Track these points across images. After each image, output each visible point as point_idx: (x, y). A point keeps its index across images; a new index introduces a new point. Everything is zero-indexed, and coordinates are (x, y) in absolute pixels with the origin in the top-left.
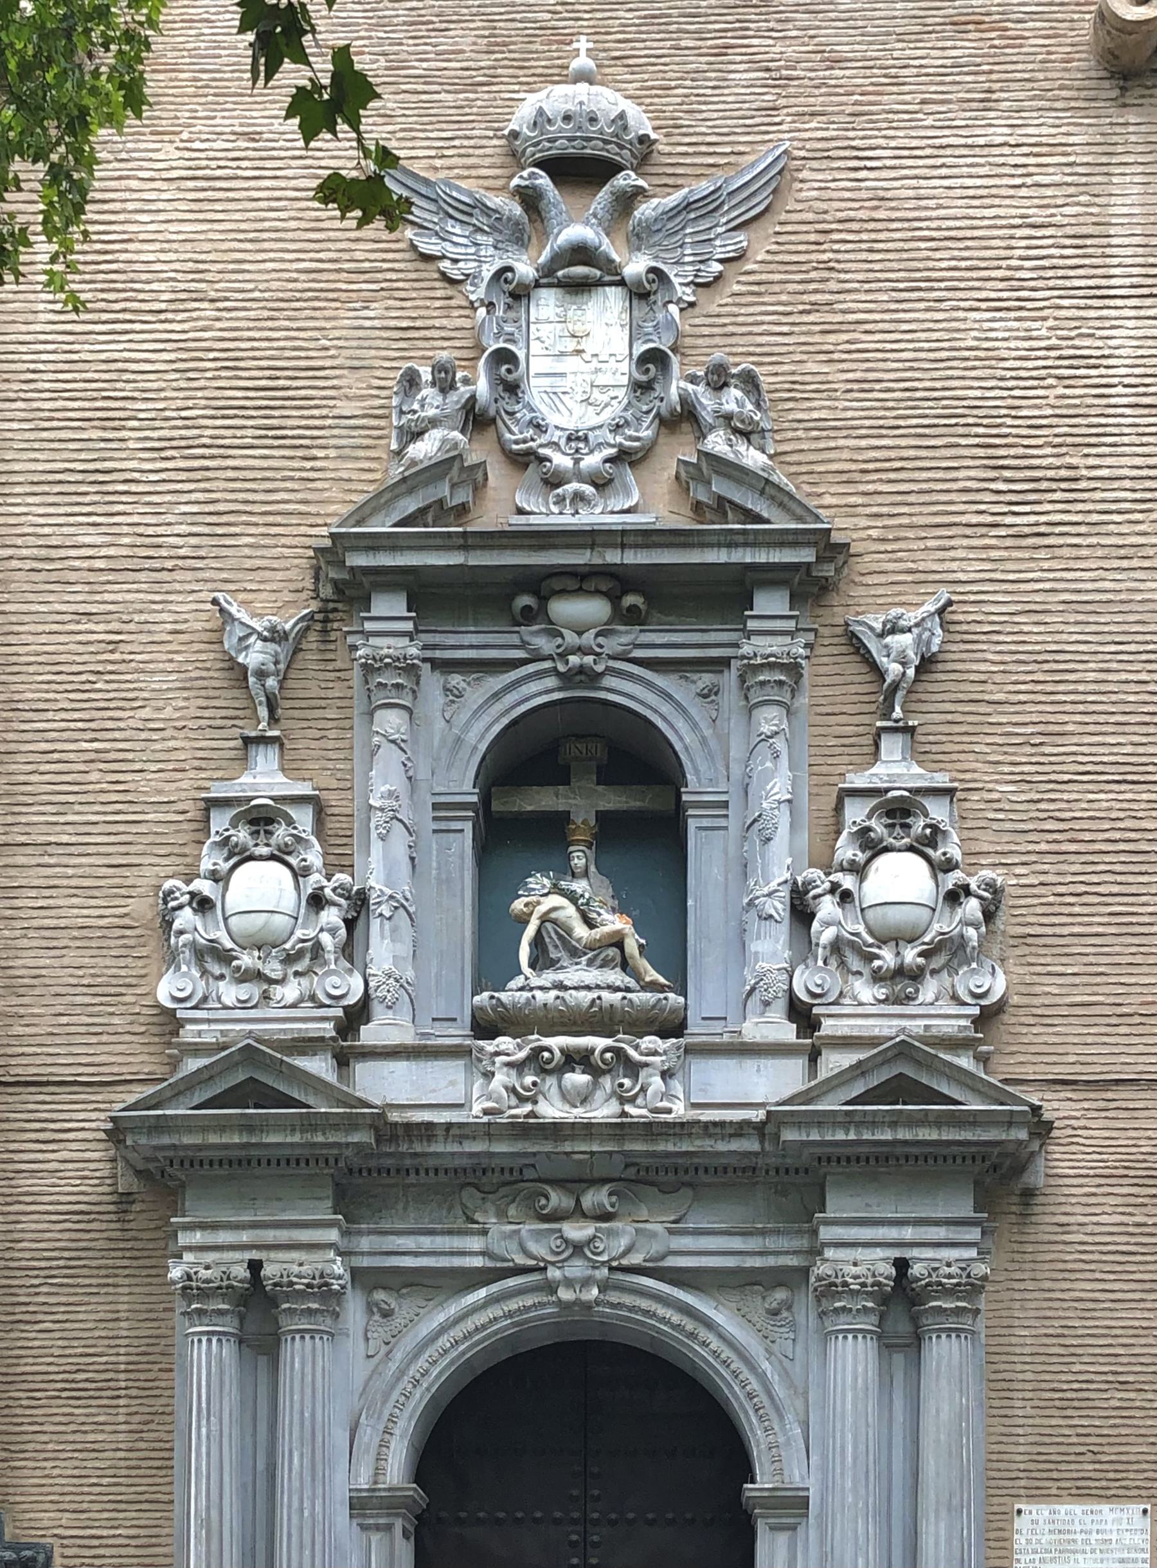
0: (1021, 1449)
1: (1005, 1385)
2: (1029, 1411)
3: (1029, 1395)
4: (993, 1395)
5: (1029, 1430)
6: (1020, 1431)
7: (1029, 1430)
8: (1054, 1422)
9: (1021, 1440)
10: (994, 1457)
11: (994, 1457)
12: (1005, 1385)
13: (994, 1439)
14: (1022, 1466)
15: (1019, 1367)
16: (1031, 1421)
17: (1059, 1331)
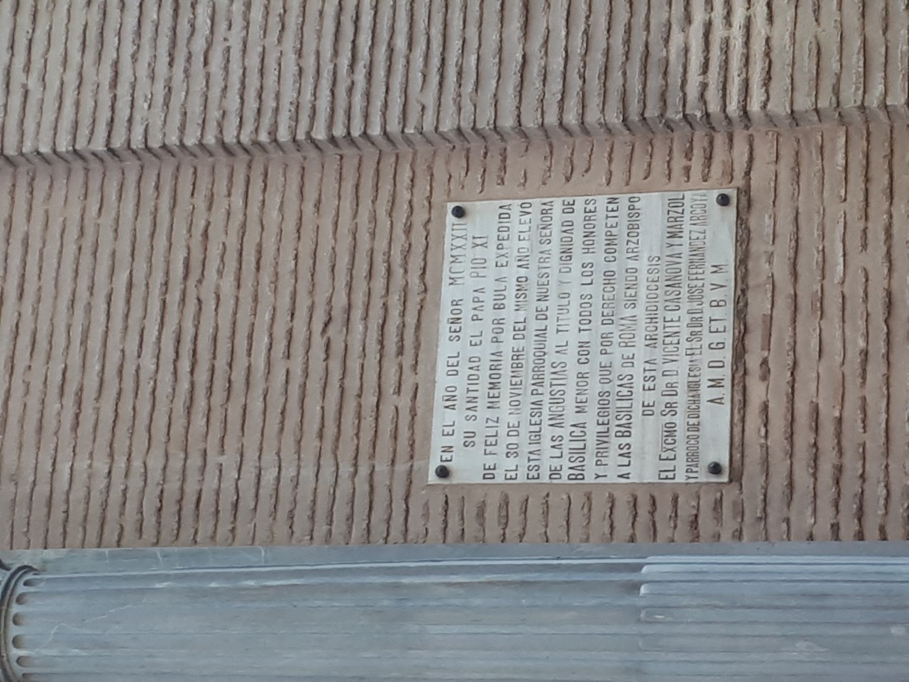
0: (308, 473)
1: (170, 508)
2: (229, 460)
3: (195, 461)
4: (187, 533)
5: (269, 457)
6: (269, 477)
7: (269, 457)
8: (256, 405)
9: (289, 472)
10: (321, 529)
11: (321, 529)
12: (170, 508)
13: (281, 529)
14: (346, 469)
15: (135, 482)
16: (251, 455)
17: (70, 400)
